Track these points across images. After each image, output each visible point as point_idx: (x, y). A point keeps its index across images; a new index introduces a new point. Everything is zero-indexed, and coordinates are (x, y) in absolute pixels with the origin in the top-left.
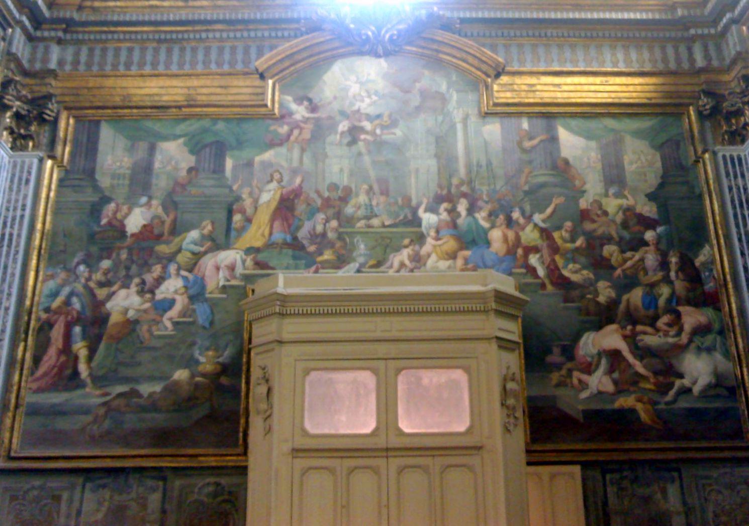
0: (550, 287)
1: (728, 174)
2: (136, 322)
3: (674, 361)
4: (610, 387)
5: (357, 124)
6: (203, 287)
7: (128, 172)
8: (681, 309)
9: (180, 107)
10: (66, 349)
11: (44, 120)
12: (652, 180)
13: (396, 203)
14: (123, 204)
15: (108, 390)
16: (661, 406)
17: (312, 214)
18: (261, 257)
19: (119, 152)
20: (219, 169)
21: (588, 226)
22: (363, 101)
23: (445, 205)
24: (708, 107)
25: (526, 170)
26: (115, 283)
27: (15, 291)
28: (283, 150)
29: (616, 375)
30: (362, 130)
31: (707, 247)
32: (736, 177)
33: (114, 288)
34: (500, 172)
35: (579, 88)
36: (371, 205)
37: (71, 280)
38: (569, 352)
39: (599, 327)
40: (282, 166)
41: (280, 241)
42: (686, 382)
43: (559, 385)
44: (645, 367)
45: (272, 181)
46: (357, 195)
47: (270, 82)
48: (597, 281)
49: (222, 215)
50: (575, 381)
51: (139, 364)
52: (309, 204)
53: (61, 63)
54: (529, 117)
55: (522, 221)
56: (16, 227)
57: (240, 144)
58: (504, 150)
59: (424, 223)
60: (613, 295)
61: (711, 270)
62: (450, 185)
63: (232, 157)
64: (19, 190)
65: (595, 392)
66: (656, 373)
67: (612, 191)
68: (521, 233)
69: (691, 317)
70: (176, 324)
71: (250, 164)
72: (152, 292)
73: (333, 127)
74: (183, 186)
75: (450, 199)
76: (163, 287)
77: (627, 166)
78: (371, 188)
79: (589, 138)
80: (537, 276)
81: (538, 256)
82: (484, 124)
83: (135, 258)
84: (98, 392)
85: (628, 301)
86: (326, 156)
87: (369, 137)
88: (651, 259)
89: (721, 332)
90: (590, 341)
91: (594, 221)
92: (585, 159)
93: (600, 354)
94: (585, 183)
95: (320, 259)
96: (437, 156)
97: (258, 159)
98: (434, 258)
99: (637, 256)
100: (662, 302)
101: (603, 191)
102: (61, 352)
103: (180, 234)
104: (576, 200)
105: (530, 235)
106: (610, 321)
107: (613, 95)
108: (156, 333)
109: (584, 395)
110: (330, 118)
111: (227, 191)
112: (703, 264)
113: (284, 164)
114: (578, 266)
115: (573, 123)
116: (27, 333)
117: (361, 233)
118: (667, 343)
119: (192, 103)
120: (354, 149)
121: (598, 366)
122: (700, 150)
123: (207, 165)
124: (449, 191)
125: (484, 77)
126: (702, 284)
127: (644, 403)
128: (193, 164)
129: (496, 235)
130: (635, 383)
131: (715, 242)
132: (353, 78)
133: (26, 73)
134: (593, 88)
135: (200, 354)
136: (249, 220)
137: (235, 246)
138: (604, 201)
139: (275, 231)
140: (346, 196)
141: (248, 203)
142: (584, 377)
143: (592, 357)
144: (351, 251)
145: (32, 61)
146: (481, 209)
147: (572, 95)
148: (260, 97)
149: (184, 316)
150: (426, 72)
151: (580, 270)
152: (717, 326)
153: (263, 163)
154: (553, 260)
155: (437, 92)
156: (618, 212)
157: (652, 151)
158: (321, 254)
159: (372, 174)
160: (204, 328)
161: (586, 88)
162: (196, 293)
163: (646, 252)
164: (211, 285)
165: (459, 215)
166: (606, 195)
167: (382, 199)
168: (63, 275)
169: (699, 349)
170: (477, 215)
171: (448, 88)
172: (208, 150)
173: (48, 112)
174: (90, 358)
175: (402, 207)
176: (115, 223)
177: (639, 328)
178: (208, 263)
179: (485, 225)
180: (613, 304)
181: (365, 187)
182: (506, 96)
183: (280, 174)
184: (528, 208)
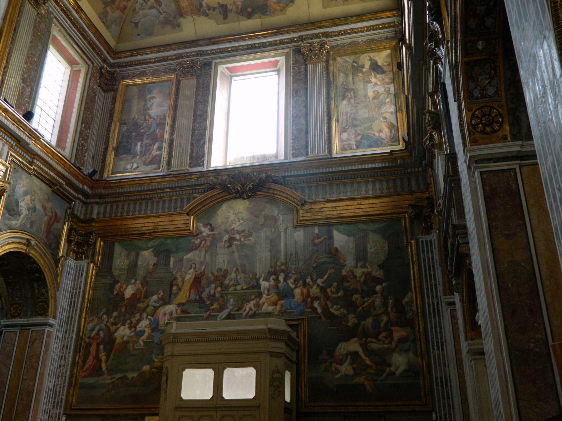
0: (323, 319)
1: (423, 252)
4: (351, 372)
5: (232, 236)
6: (158, 324)
8: (392, 328)
9: (150, 233)
10: (97, 357)
12: (382, 257)
14: (124, 284)
15: (114, 376)
17: (209, 285)
18: (184, 308)
20: (167, 264)
21: (346, 284)
22: (236, 224)
23: (273, 277)
24: (413, 214)
25: (315, 256)
26: (119, 323)
27: (75, 329)
28: (197, 252)
29: (355, 366)
30: (234, 239)
31: (410, 293)
32: (428, 252)
33: (119, 326)
35: (346, 208)
36: (237, 279)
37: (100, 322)
38: (331, 353)
39: (347, 339)
41: (194, 299)
42: (392, 369)
45: (191, 269)
46: (230, 274)
47: (192, 217)
48: (348, 314)
50: (333, 369)
53: (98, 214)
54: (318, 226)
55: (311, 283)
56: (77, 297)
59: (262, 287)
61: (411, 306)
64: (78, 280)
65: (343, 374)
67: (359, 265)
68: (310, 290)
69: (398, 333)
70: (145, 343)
71: (181, 260)
72: (136, 328)
73: (221, 239)
74: (151, 273)
76: (140, 325)
77: (368, 250)
78: (237, 269)
80: (317, 313)
81: (318, 302)
83: (128, 311)
84: (109, 377)
85: (364, 324)
86: (217, 254)
87: (238, 243)
88: (378, 301)
90: (342, 347)
91: (348, 282)
94: (345, 261)
95: (212, 308)
97: (185, 257)
98: (266, 304)
99: (370, 301)
101: (355, 264)
103: (148, 298)
105: (315, 291)
108: (136, 348)
109: (337, 376)
110: (220, 234)
111: (170, 274)
112: (407, 303)
113: (197, 259)
114: (339, 306)
115: (341, 227)
116: (80, 349)
117: (232, 293)
119: (156, 230)
120: (230, 249)
122: (409, 237)
123: (162, 262)
124: (276, 269)
125: (296, 206)
129: (298, 291)
131: (413, 290)
132: (232, 211)
134: (353, 207)
135: (155, 358)
137: (173, 303)
138: (355, 270)
139: (191, 294)
141: (180, 280)
142: (338, 366)
145: (85, 214)
146: (291, 278)
147: (342, 212)
148: (187, 225)
149: (149, 339)
150: (268, 206)
151: (340, 308)
153: (187, 259)
154: (326, 304)
155: (272, 216)
158: (212, 305)
159: (238, 262)
160: (157, 344)
161: (350, 207)
163: (376, 297)
165: (280, 281)
167: (243, 275)
168: (96, 320)
169: (401, 351)
170: (289, 281)
171: (278, 213)
172: (163, 254)
173: (91, 240)
176: (120, 293)
177: (369, 339)
178: (161, 311)
179: (293, 286)
180: (356, 326)
181: (235, 269)
182: (308, 216)
183: (195, 264)
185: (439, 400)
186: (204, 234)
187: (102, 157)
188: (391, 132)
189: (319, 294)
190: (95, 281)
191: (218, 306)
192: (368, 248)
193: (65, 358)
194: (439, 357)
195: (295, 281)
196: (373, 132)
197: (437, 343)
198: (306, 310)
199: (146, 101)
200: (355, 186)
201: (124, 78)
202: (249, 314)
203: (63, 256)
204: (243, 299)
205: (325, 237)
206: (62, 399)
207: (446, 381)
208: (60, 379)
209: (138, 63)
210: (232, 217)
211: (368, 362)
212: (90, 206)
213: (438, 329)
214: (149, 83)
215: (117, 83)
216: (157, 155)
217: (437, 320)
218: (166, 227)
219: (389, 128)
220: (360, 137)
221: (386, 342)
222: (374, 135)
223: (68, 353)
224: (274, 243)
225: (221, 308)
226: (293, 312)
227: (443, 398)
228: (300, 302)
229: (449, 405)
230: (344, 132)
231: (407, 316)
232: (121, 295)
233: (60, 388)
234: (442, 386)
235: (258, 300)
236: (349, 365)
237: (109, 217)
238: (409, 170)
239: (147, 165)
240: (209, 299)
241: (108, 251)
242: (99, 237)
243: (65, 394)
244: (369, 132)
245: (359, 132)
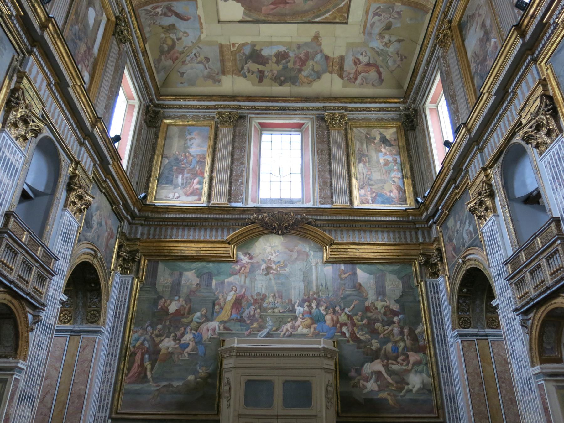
0: (351, 342)
1: (431, 292)
2: (172, 353)
3: (405, 377)
4: (376, 388)
5: (269, 265)
6: (202, 338)
7: (170, 285)
8: (408, 353)
10: (142, 365)
11: (135, 261)
12: (398, 294)
14: (168, 300)
15: (159, 384)
16: (399, 398)
17: (249, 306)
18: (227, 325)
20: (210, 285)
21: (369, 314)
23: (306, 304)
24: (423, 261)
25: (342, 288)
28: (237, 277)
29: (379, 383)
31: (421, 325)
32: (434, 293)
34: (331, 288)
35: (366, 251)
37: (145, 333)
38: (358, 371)
39: (372, 360)
40: (236, 284)
41: (235, 318)
42: (410, 387)
43: (353, 387)
44: (392, 379)
46: (269, 298)
49: (211, 305)
52: (248, 302)
53: (142, 234)
55: (340, 311)
57: (218, 274)
58: (333, 278)
60: (379, 346)
64: (123, 292)
65: (370, 390)
66: (397, 382)
67: (379, 298)
68: (339, 317)
69: (414, 357)
70: (189, 354)
71: (223, 283)
72: (180, 340)
73: (259, 266)
74: (194, 292)
75: (309, 301)
76: (184, 338)
78: (275, 295)
79: (370, 273)
80: (346, 337)
81: (346, 327)
84: (155, 385)
85: (385, 349)
86: (256, 280)
87: (274, 272)
88: (396, 330)
89: (426, 364)
90: (368, 367)
91: (371, 312)
92: (368, 283)
93: (372, 373)
94: (368, 295)
96: (304, 281)
97: (226, 280)
98: (301, 327)
99: (390, 329)
104: (364, 302)
105: (343, 318)
106: (377, 358)
107: (382, 254)
108: (181, 358)
110: (258, 262)
111: (213, 295)
112: (419, 333)
113: (238, 283)
114: (364, 332)
115: (363, 266)
117: (270, 315)
118: (402, 368)
120: (268, 277)
122: (419, 280)
124: (309, 297)
125: (325, 245)
126: (418, 342)
127: (391, 396)
128: (198, 282)
129: (328, 317)
130: (388, 387)
131: (424, 323)
132: (268, 244)
133: (128, 240)
134: (373, 251)
136: (222, 308)
138: (376, 303)
139: (233, 313)
140: (264, 297)
141: (222, 300)
142: (365, 383)
143: (369, 374)
144: (266, 323)
145: (130, 234)
146: (322, 305)
148: (228, 252)
150: (300, 242)
152: (424, 362)
153: (228, 282)
154: (353, 330)
155: (304, 251)
156: (382, 308)
157: (398, 280)
158: (252, 324)
159: (275, 288)
160: (202, 356)
161: (370, 251)
162: (198, 340)
163: (394, 327)
164: (205, 337)
165: (313, 307)
166: (377, 301)
167: (279, 300)
168: (141, 331)
169: (416, 372)
170: (320, 308)
171: (310, 250)
172: (205, 276)
173: (137, 257)
174: (152, 369)
176: (164, 308)
177: (390, 361)
178: (204, 327)
179: (324, 313)
180: (379, 350)
181: (272, 294)
183: (236, 287)
184: (342, 305)
185: (449, 414)
186: (244, 262)
187: (145, 184)
188: (399, 193)
189: (347, 321)
190: (139, 295)
193: (110, 365)
194: (447, 379)
195: (326, 308)
196: (385, 192)
197: (445, 366)
198: (336, 334)
199: (186, 140)
201: (165, 118)
202: (286, 335)
203: (113, 270)
204: (281, 321)
205: (350, 273)
206: (107, 403)
207: (454, 398)
208: (105, 384)
209: (180, 107)
210: (269, 249)
211: (390, 380)
212: (134, 227)
213: (445, 355)
214: (189, 126)
215: (159, 122)
216: (197, 189)
217: (444, 348)
218: (208, 252)
220: (374, 194)
221: (404, 364)
223: (113, 360)
224: (306, 275)
225: (261, 328)
226: (325, 335)
227: (452, 412)
228: (331, 326)
229: (457, 418)
230: (362, 188)
231: (420, 343)
232: (165, 310)
233: (106, 393)
234: (451, 402)
235: (294, 322)
236: (374, 382)
237: (152, 238)
238: (417, 226)
239: (188, 196)
240: (249, 319)
241: (152, 270)
242: (144, 255)
243: (110, 399)
244: (382, 191)
245: (374, 190)
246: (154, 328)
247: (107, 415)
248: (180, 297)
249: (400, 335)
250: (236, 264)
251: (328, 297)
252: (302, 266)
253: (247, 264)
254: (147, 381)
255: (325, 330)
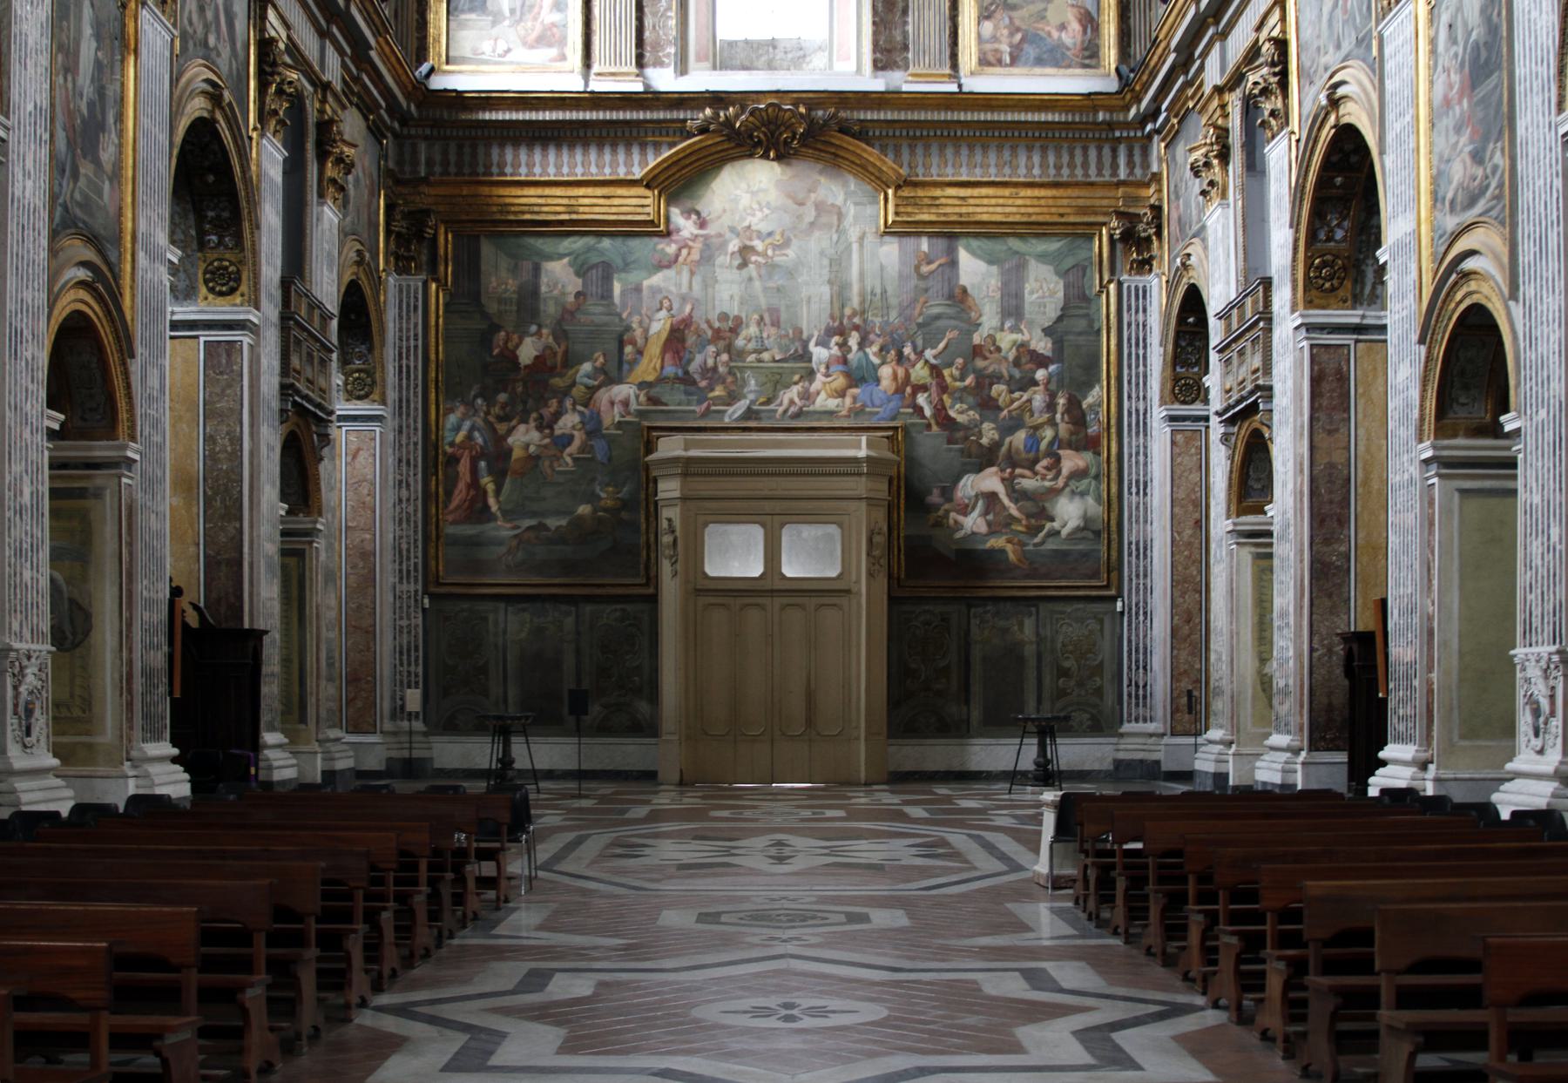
0: (935, 428)
1: (1129, 309)
5: (748, 243)
6: (600, 422)
7: (515, 296)
10: (475, 483)
11: (424, 238)
12: (1052, 312)
13: (787, 336)
17: (702, 347)
18: (654, 392)
19: (504, 274)
20: (607, 295)
21: (980, 363)
22: (754, 215)
23: (836, 339)
25: (922, 300)
27: (420, 426)
28: (670, 273)
29: (990, 517)
30: (751, 249)
31: (1097, 388)
32: (1137, 311)
33: (514, 422)
34: (893, 301)
38: (948, 493)
39: (979, 469)
40: (670, 292)
42: (1056, 525)
44: (1019, 509)
45: (661, 309)
46: (748, 326)
48: (982, 423)
49: (613, 346)
51: (544, 499)
53: (430, 163)
55: (913, 357)
56: (412, 358)
57: (626, 267)
58: (901, 276)
60: (997, 437)
61: (1098, 413)
62: (842, 316)
63: (620, 280)
66: (1028, 516)
67: (1008, 325)
68: (911, 371)
69: (1071, 461)
70: (575, 460)
71: (638, 289)
72: (552, 429)
73: (723, 245)
74: (572, 313)
75: (842, 332)
76: (561, 423)
77: (1026, 295)
78: (762, 318)
79: (990, 262)
80: (923, 417)
81: (926, 395)
82: (882, 244)
84: (509, 525)
86: (716, 281)
87: (760, 259)
88: (1038, 399)
89: (1097, 477)
90: (969, 483)
91: (986, 358)
93: (977, 496)
94: (981, 316)
95: (711, 395)
96: (830, 282)
98: (823, 395)
99: (1025, 398)
100: (1043, 445)
102: (469, 487)
103: (572, 367)
104: (970, 333)
105: (920, 373)
110: (720, 235)
111: (617, 320)
112: (1090, 406)
113: (673, 289)
114: (965, 406)
115: (975, 243)
116: (436, 467)
117: (752, 368)
120: (745, 272)
121: (973, 508)
122: (1106, 277)
124: (841, 323)
126: (1086, 428)
128: (580, 289)
129: (886, 372)
130: (1008, 525)
131: (1105, 383)
132: (743, 185)
134: (1001, 201)
136: (640, 353)
138: (998, 336)
141: (638, 333)
142: (960, 518)
143: (970, 499)
146: (872, 343)
147: (979, 210)
149: (583, 452)
150: (823, 180)
151: (967, 410)
152: (1093, 471)
153: (651, 287)
154: (941, 400)
155: (833, 205)
157: (1055, 278)
158: (712, 390)
161: (993, 201)
162: (593, 428)
163: (1035, 393)
164: (607, 421)
165: (850, 349)
166: (1002, 330)
167: (773, 331)
168: (461, 409)
169: (1073, 493)
170: (868, 350)
171: (845, 201)
174: (498, 492)
175: (792, 341)
177: (1018, 471)
178: (603, 396)
179: (876, 361)
180: (996, 445)
181: (756, 317)
184: (920, 342)
185: (1131, 580)
186: (685, 234)
187: (416, 16)
188: (1085, 32)
189: (928, 380)
190: (445, 323)
191: (723, 393)
192: (1026, 291)
193: (408, 485)
194: (1137, 508)
195: (881, 350)
196: (1047, 28)
197: (1137, 482)
198: (902, 410)
200: (1007, 154)
204: (778, 382)
205: (942, 261)
206: (416, 564)
207: (1145, 549)
208: (404, 525)
210: (745, 200)
211: (1014, 511)
213: (1141, 458)
216: (554, 25)
217: (1141, 440)
218: (597, 209)
219: (1080, 21)
220: (1018, 37)
222: (1049, 34)
223: (412, 473)
225: (732, 398)
226: (877, 413)
227: (1138, 576)
229: (1145, 588)
230: (988, 18)
231: (1090, 431)
232: (511, 358)
233: (409, 543)
234: (1138, 557)
235: (807, 384)
237: (456, 175)
238: (1117, 134)
239: (532, 47)
240: (704, 378)
242: (442, 221)
243: (420, 554)
244: (1040, 26)
245: (1017, 23)
246: (490, 401)
247: (420, 587)
248: (540, 327)
249: (1048, 412)
250: (667, 240)
251: (887, 322)
252: (825, 244)
253: (693, 241)
254: (491, 518)
255: (877, 402)
